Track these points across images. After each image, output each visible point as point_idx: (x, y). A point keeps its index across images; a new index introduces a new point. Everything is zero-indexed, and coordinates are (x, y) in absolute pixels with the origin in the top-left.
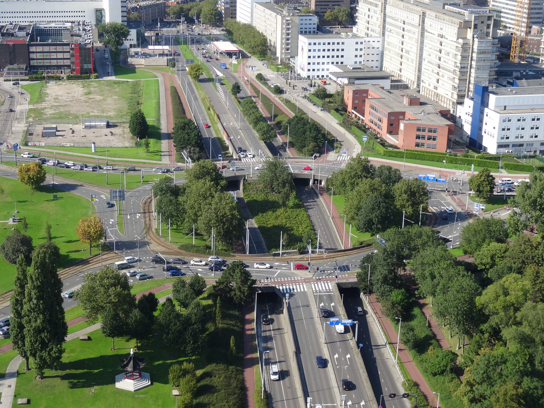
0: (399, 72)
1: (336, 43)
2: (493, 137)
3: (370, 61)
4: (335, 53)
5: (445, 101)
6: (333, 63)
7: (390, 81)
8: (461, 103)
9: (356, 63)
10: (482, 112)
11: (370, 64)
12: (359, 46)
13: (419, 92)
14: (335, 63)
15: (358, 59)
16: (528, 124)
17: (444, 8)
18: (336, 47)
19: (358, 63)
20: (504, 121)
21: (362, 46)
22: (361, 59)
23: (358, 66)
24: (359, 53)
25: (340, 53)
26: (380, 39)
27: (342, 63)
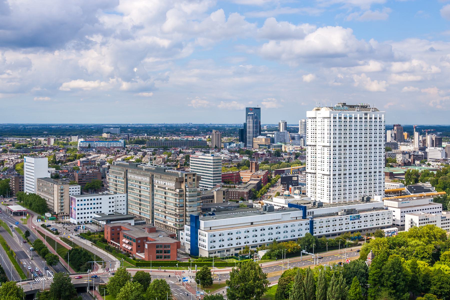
0: (139, 215)
1: (96, 199)
2: (205, 247)
3: (122, 201)
4: (96, 206)
5: (171, 229)
6: (94, 212)
7: (134, 220)
8: (183, 230)
9: (110, 211)
10: (197, 233)
11: (120, 211)
12: (111, 200)
13: (154, 225)
14: (96, 213)
15: (112, 209)
16: (226, 237)
17: (165, 171)
18: (96, 202)
19: (111, 211)
20: (211, 236)
21: (113, 200)
22: (113, 209)
23: (111, 213)
24: (111, 205)
25: (99, 206)
26: (125, 195)
27: (101, 212)
